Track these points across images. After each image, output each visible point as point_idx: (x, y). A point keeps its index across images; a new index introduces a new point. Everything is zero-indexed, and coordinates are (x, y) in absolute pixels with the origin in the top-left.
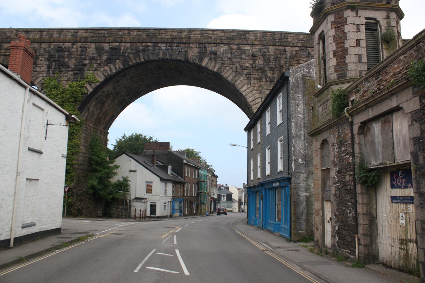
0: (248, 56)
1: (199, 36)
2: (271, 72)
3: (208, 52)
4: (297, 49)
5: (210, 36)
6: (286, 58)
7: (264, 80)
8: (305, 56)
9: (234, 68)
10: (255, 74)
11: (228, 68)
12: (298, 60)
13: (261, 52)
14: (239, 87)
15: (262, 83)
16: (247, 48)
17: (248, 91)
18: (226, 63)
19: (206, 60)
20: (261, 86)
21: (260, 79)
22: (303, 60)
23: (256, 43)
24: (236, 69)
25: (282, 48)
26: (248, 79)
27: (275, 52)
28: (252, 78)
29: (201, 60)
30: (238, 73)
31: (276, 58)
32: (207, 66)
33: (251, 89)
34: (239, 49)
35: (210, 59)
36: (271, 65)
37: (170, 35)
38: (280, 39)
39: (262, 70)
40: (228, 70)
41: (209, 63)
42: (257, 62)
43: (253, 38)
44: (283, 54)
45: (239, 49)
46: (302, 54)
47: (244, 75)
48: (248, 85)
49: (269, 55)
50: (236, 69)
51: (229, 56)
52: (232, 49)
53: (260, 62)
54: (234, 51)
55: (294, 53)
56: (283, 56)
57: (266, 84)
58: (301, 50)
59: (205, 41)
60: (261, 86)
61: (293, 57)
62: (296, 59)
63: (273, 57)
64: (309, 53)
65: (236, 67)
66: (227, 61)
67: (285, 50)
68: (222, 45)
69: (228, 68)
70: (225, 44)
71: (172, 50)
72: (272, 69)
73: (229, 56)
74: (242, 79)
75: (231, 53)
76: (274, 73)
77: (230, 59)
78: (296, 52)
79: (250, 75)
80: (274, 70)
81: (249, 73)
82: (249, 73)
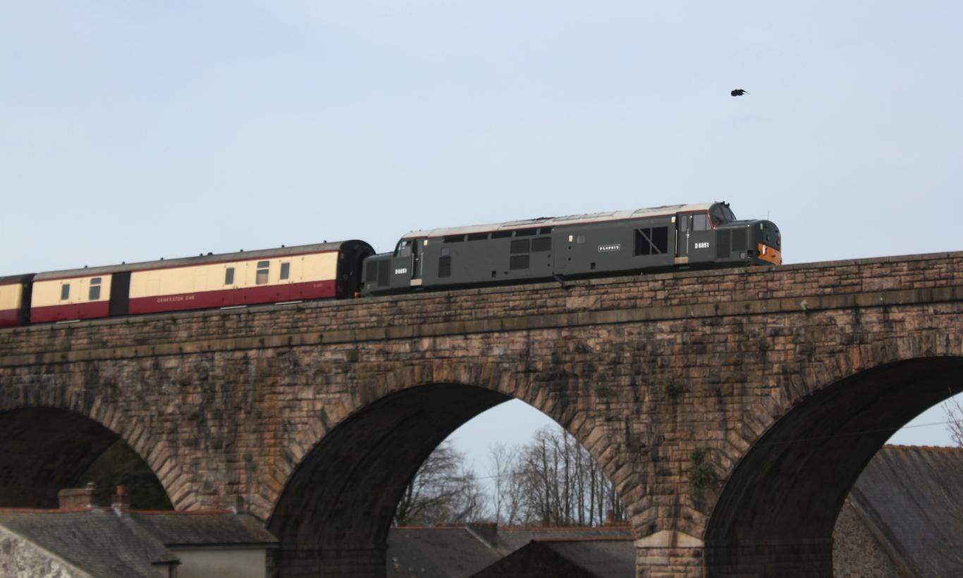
0: (174, 383)
1: (85, 341)
2: (217, 422)
3: (102, 381)
4: (270, 353)
5: (105, 339)
6: (246, 382)
7: (203, 446)
8: (287, 371)
9: (147, 419)
10: (187, 432)
11: (134, 420)
12: (274, 385)
13: (198, 371)
14: (155, 468)
15: (199, 454)
16: (172, 363)
17: (171, 476)
18: (132, 407)
19: (98, 403)
20: (196, 463)
21: (193, 444)
22: (283, 382)
23: (189, 348)
24: (151, 421)
25: (239, 355)
26: (173, 443)
27: (224, 368)
28: (180, 443)
29: (89, 403)
30: (154, 435)
31: (228, 387)
32: (99, 419)
33: (176, 471)
34: (156, 366)
35: (105, 401)
36: (218, 402)
37: (37, 345)
38: (238, 329)
39: (197, 419)
40: (136, 425)
41: (103, 411)
42: (190, 399)
43: (183, 334)
44: (241, 372)
45: (156, 366)
46: (282, 366)
47: (164, 437)
48: (171, 462)
49: (214, 377)
50: (151, 421)
51: (139, 387)
52: (144, 370)
53: (195, 399)
54: (147, 374)
55: (265, 364)
56: (242, 378)
57: (205, 455)
58: (280, 354)
59: (94, 353)
60: (196, 463)
61: (262, 376)
62: (270, 381)
63: (222, 382)
64: (296, 364)
65: (152, 416)
66: (135, 401)
67: (246, 360)
68: (125, 362)
69: (134, 420)
70: (131, 359)
71: (39, 381)
72: (218, 415)
73: (139, 387)
74: (160, 445)
75: (143, 380)
76: (221, 426)
77: (140, 397)
78: (270, 361)
79: (175, 435)
80: (221, 418)
81: (174, 431)
82: (174, 431)
